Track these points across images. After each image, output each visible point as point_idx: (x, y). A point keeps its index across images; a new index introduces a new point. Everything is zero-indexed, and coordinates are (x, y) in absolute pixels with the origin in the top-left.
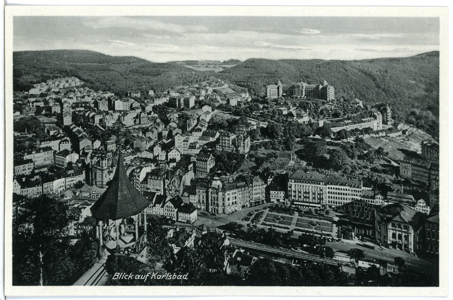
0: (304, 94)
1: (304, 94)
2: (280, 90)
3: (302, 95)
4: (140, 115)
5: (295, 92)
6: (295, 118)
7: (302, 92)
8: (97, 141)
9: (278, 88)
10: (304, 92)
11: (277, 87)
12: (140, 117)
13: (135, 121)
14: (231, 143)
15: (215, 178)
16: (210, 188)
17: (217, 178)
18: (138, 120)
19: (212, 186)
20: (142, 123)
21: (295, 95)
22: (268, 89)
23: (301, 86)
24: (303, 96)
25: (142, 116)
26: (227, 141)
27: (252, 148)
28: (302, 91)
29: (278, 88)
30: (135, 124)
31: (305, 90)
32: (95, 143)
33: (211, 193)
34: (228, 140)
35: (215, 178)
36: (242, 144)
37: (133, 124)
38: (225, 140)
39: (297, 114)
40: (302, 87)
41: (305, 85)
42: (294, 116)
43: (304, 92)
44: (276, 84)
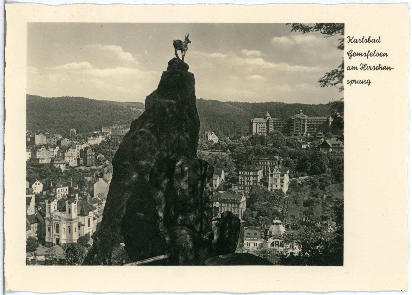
0: (306, 129)
1: (306, 129)
2: (270, 126)
3: (304, 131)
4: (85, 152)
5: (293, 128)
6: (331, 150)
7: (304, 128)
8: (37, 182)
9: (268, 123)
10: (306, 126)
11: (265, 121)
12: (85, 155)
13: (78, 162)
14: (259, 181)
15: (275, 221)
16: (271, 236)
17: (279, 221)
18: (82, 161)
19: (273, 234)
20: (87, 164)
21: (293, 131)
22: (254, 125)
23: (301, 118)
24: (305, 133)
25: (88, 154)
26: (252, 178)
27: (292, 185)
28: (304, 125)
29: (268, 123)
30: (79, 165)
31: (307, 125)
32: (34, 186)
33: (272, 244)
34: (254, 176)
35: (275, 221)
36: (279, 181)
37: (76, 165)
38: (249, 176)
39: (332, 145)
40: (304, 120)
41: (306, 117)
42: (329, 147)
43: (306, 126)
44: (265, 118)
